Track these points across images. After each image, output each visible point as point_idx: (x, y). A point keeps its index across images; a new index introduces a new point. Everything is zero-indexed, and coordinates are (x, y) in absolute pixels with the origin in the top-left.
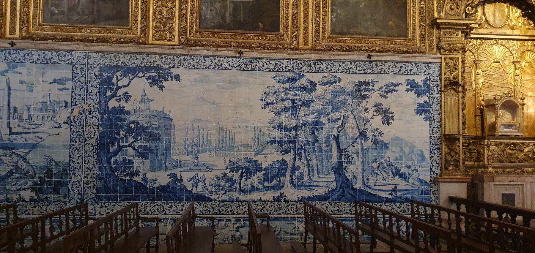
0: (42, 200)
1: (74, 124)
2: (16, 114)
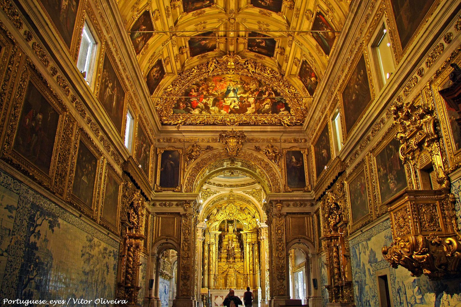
1: (10, 253)
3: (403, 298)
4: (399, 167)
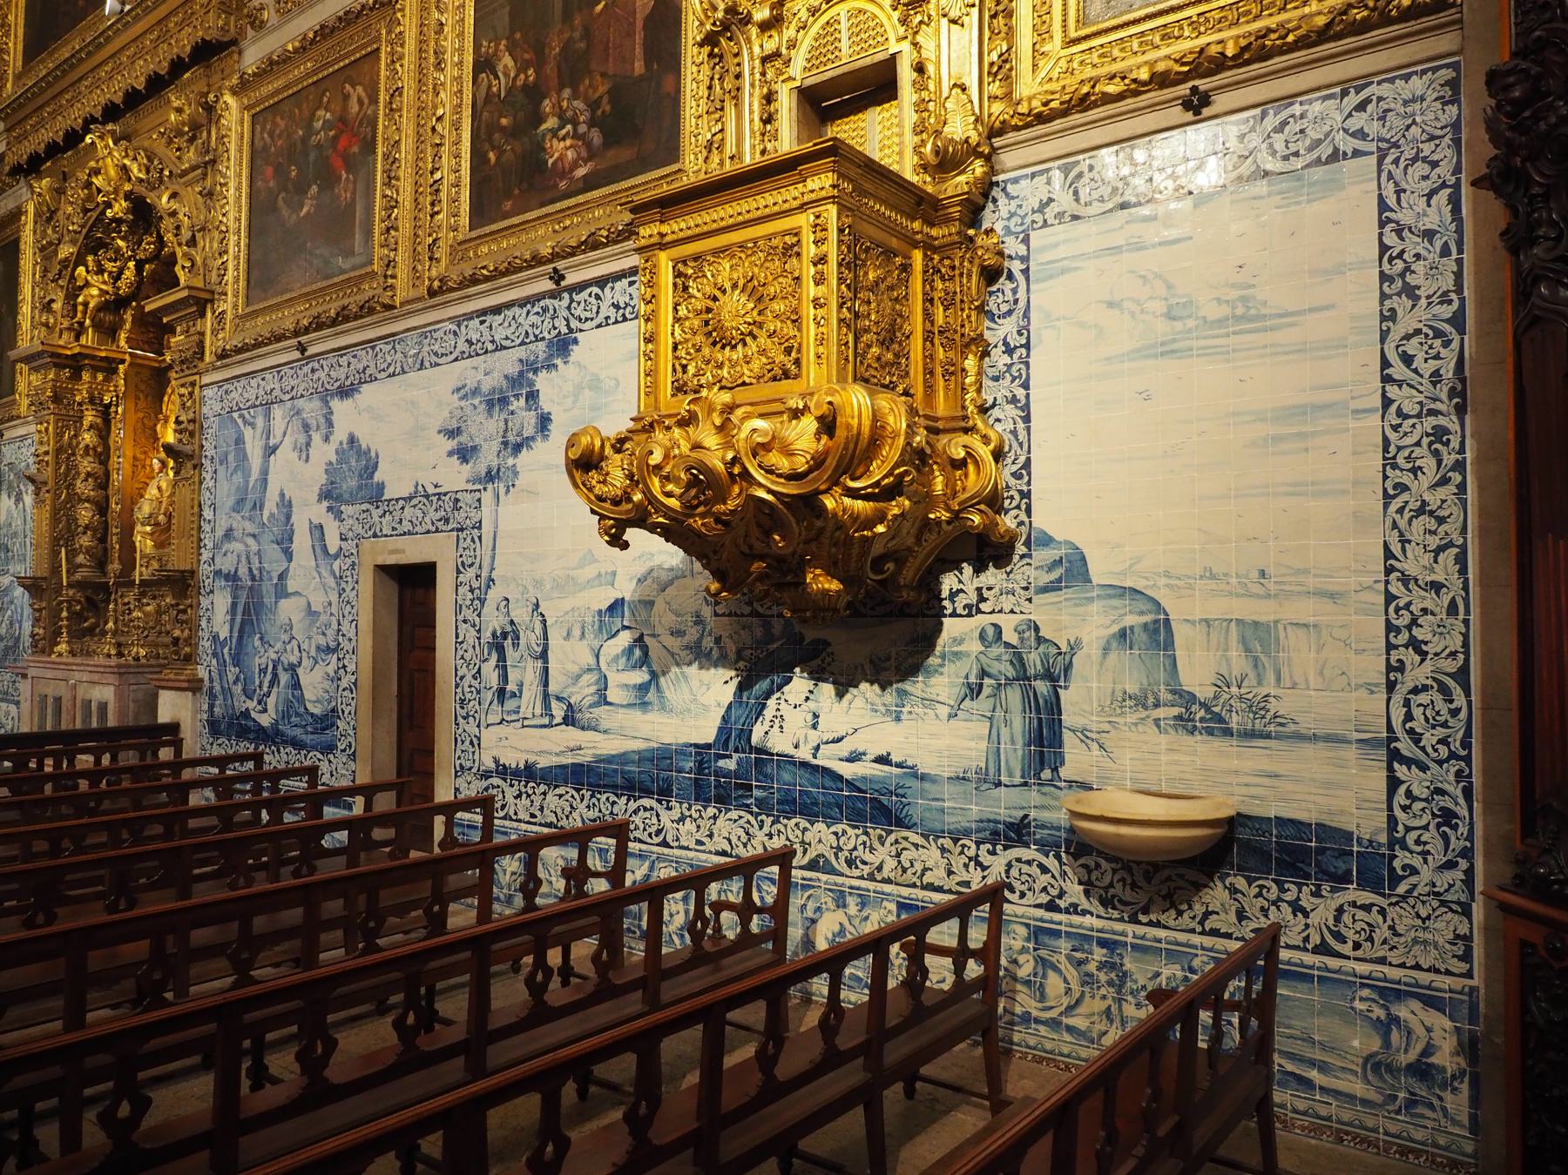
3: (524, 673)
4: (639, 67)
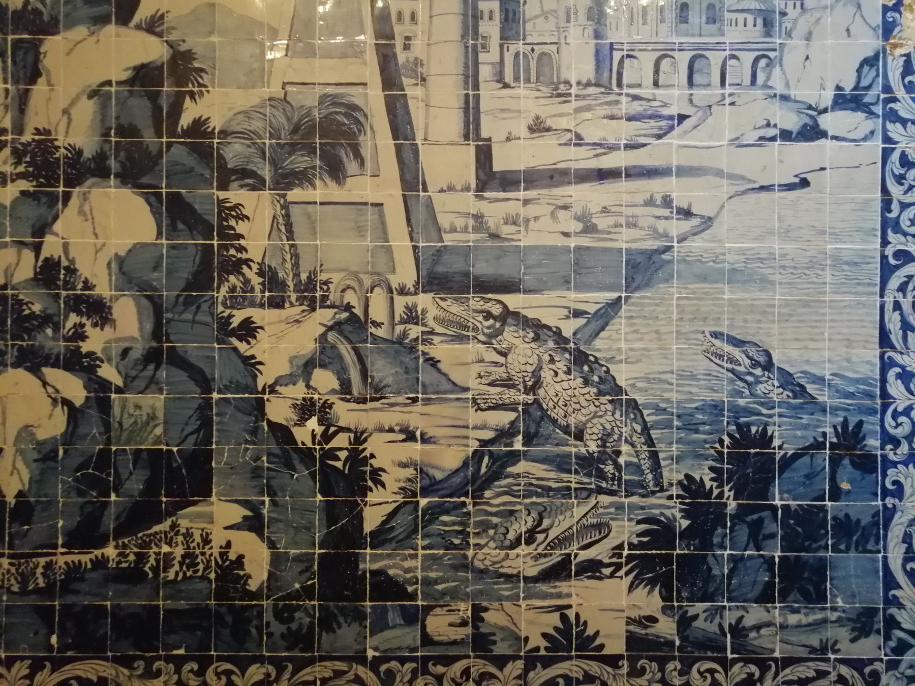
0: (710, 646)
2: (520, 47)
